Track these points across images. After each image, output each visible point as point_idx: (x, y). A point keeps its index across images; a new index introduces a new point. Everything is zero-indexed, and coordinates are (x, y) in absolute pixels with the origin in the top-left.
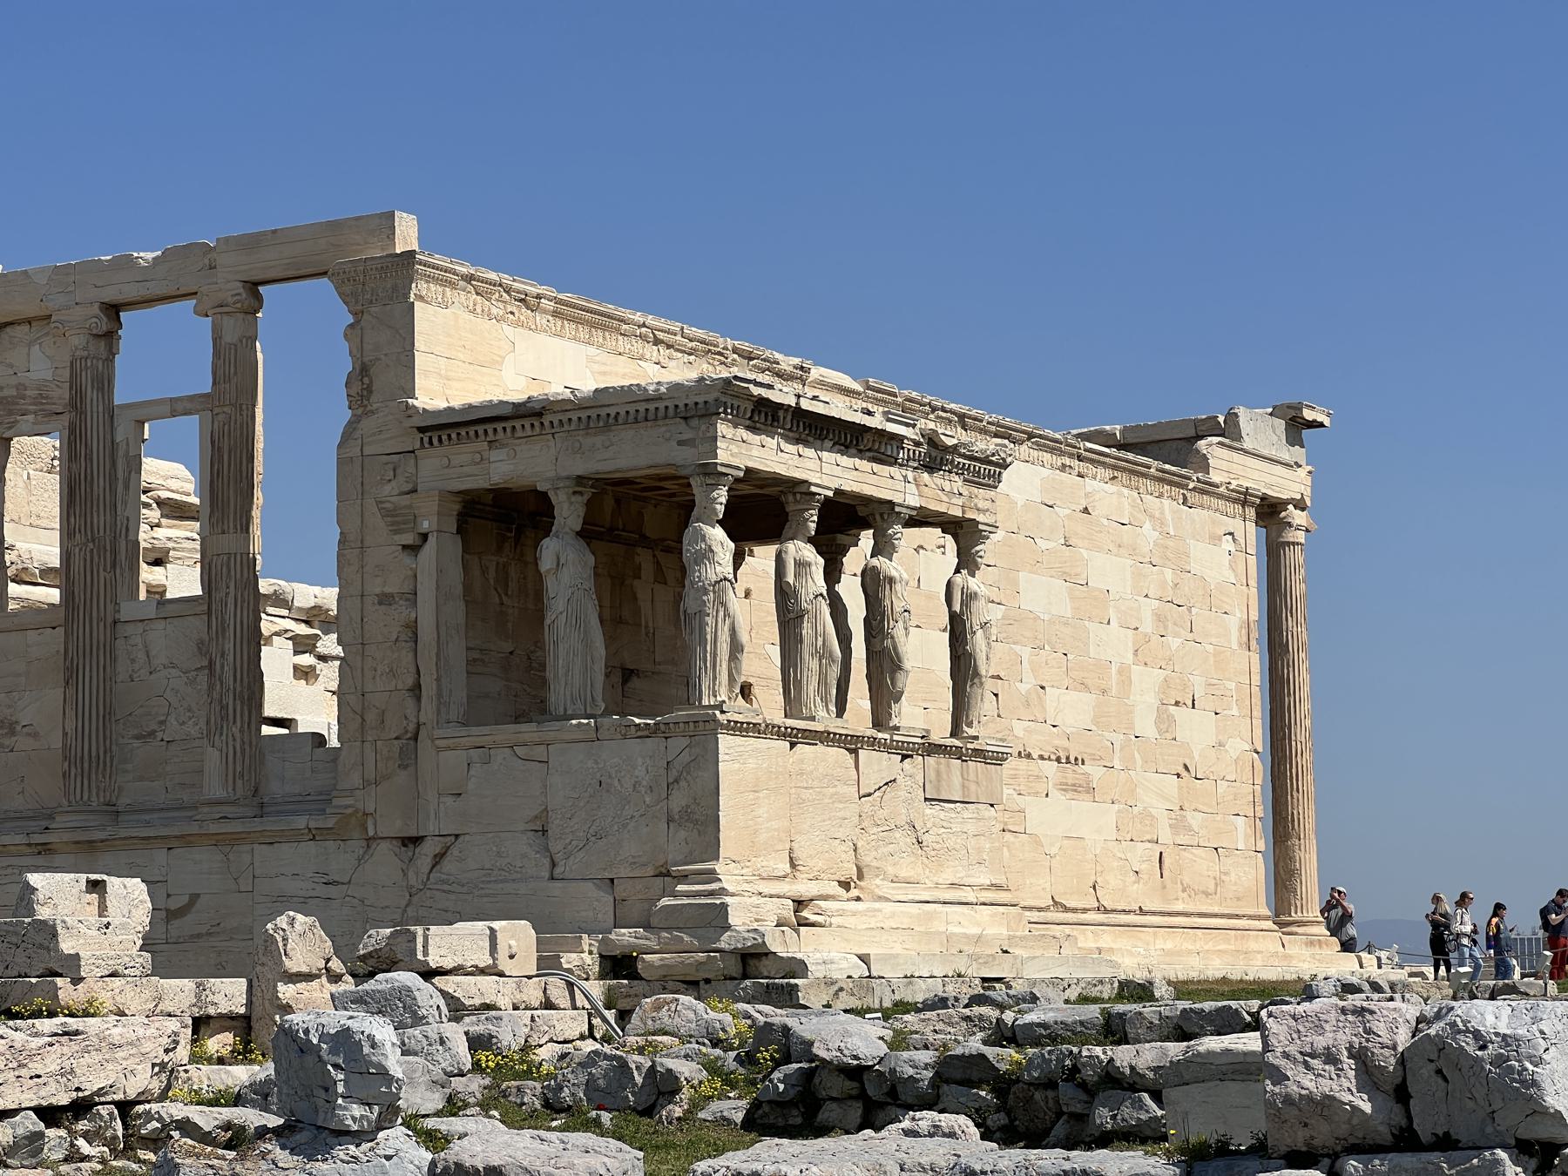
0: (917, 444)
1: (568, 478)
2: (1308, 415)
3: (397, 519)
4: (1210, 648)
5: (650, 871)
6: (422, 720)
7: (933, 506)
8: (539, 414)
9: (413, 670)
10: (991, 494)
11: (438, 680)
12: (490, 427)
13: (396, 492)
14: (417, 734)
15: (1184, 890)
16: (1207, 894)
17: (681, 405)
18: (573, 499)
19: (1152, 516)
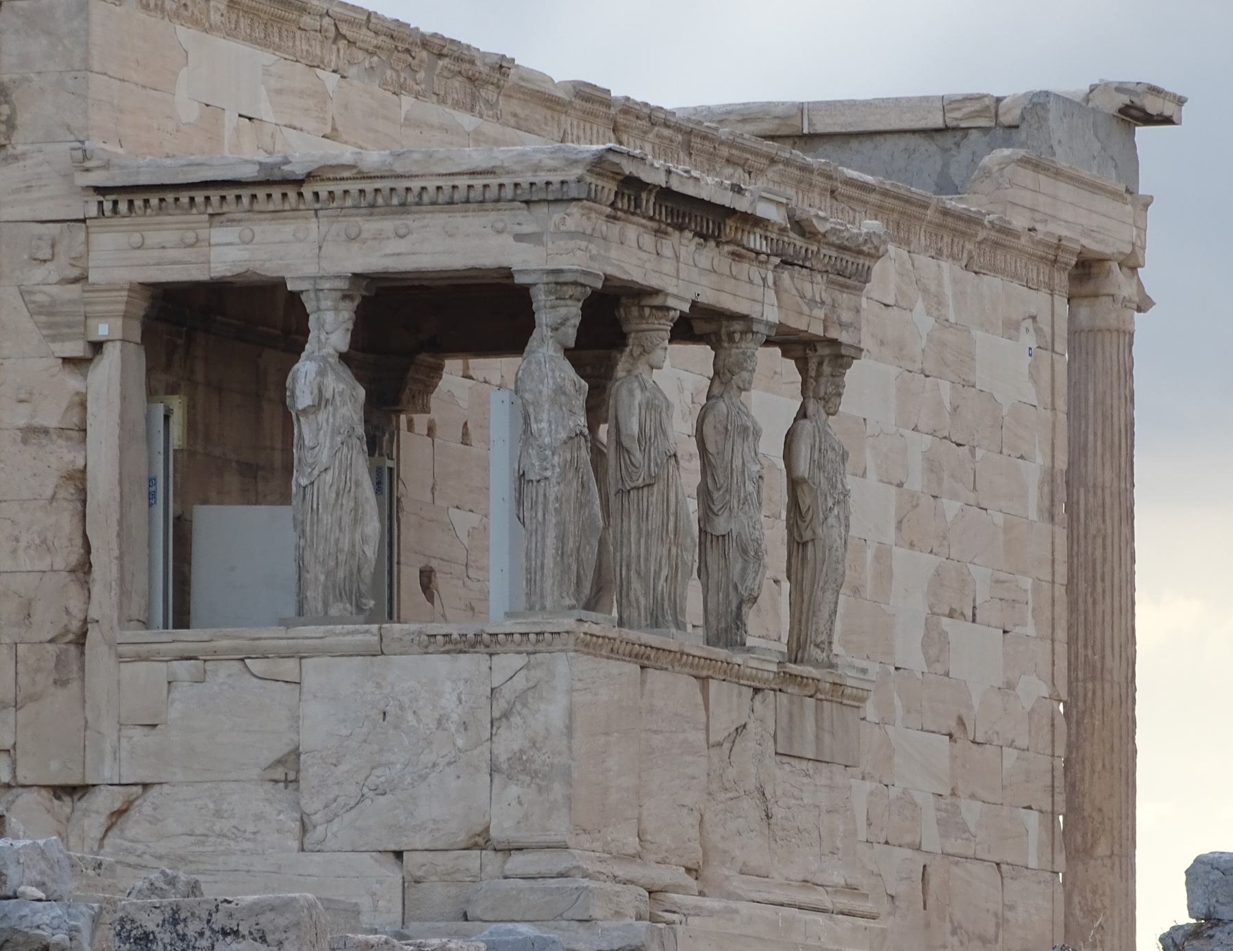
0: (783, 230)
1: (338, 277)
2: (1153, 106)
3: (51, 319)
4: (999, 518)
5: (462, 838)
6: (94, 613)
9: (79, 541)
12: (215, 195)
13: (55, 277)
14: (84, 634)
15: (954, 933)
16: (984, 940)
17: (526, 186)
18: (342, 305)
19: (925, 291)
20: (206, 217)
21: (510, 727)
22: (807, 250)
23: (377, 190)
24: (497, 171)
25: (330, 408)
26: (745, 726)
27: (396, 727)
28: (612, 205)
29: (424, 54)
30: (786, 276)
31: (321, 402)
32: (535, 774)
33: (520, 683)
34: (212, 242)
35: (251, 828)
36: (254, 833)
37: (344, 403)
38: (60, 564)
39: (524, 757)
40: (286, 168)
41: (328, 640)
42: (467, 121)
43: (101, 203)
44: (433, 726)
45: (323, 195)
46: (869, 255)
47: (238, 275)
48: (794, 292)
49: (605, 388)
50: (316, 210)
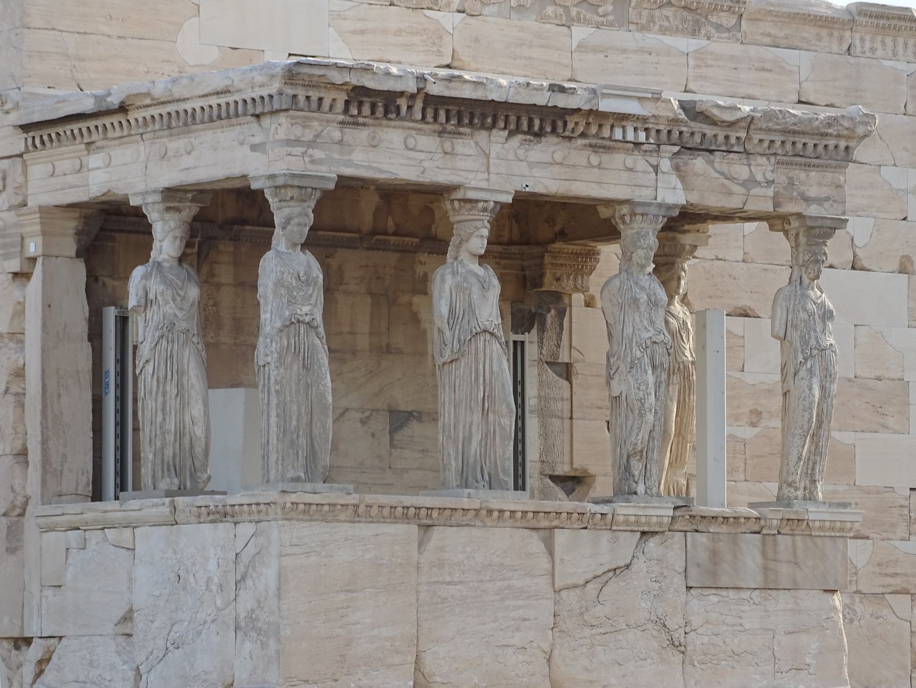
0: (675, 121)
1: (154, 192)
6: (29, 492)
7: (714, 201)
8: (123, 109)
10: (829, 175)
11: (44, 442)
12: (83, 125)
18: (167, 216)
20: (83, 146)
21: (245, 588)
22: (727, 137)
23: (169, 114)
24: (232, 89)
25: (155, 307)
26: (627, 566)
27: (184, 589)
28: (346, 111)
30: (699, 163)
31: (147, 302)
32: (259, 631)
33: (251, 549)
34: (90, 167)
35: (108, 677)
36: (110, 681)
37: (167, 303)
38: (8, 451)
39: (254, 616)
40: (109, 99)
41: (145, 512)
42: (684, 43)
43: (26, 139)
44: (204, 588)
45: (140, 120)
46: (838, 136)
47: (104, 194)
48: (717, 175)
49: (673, 264)
50: (142, 134)
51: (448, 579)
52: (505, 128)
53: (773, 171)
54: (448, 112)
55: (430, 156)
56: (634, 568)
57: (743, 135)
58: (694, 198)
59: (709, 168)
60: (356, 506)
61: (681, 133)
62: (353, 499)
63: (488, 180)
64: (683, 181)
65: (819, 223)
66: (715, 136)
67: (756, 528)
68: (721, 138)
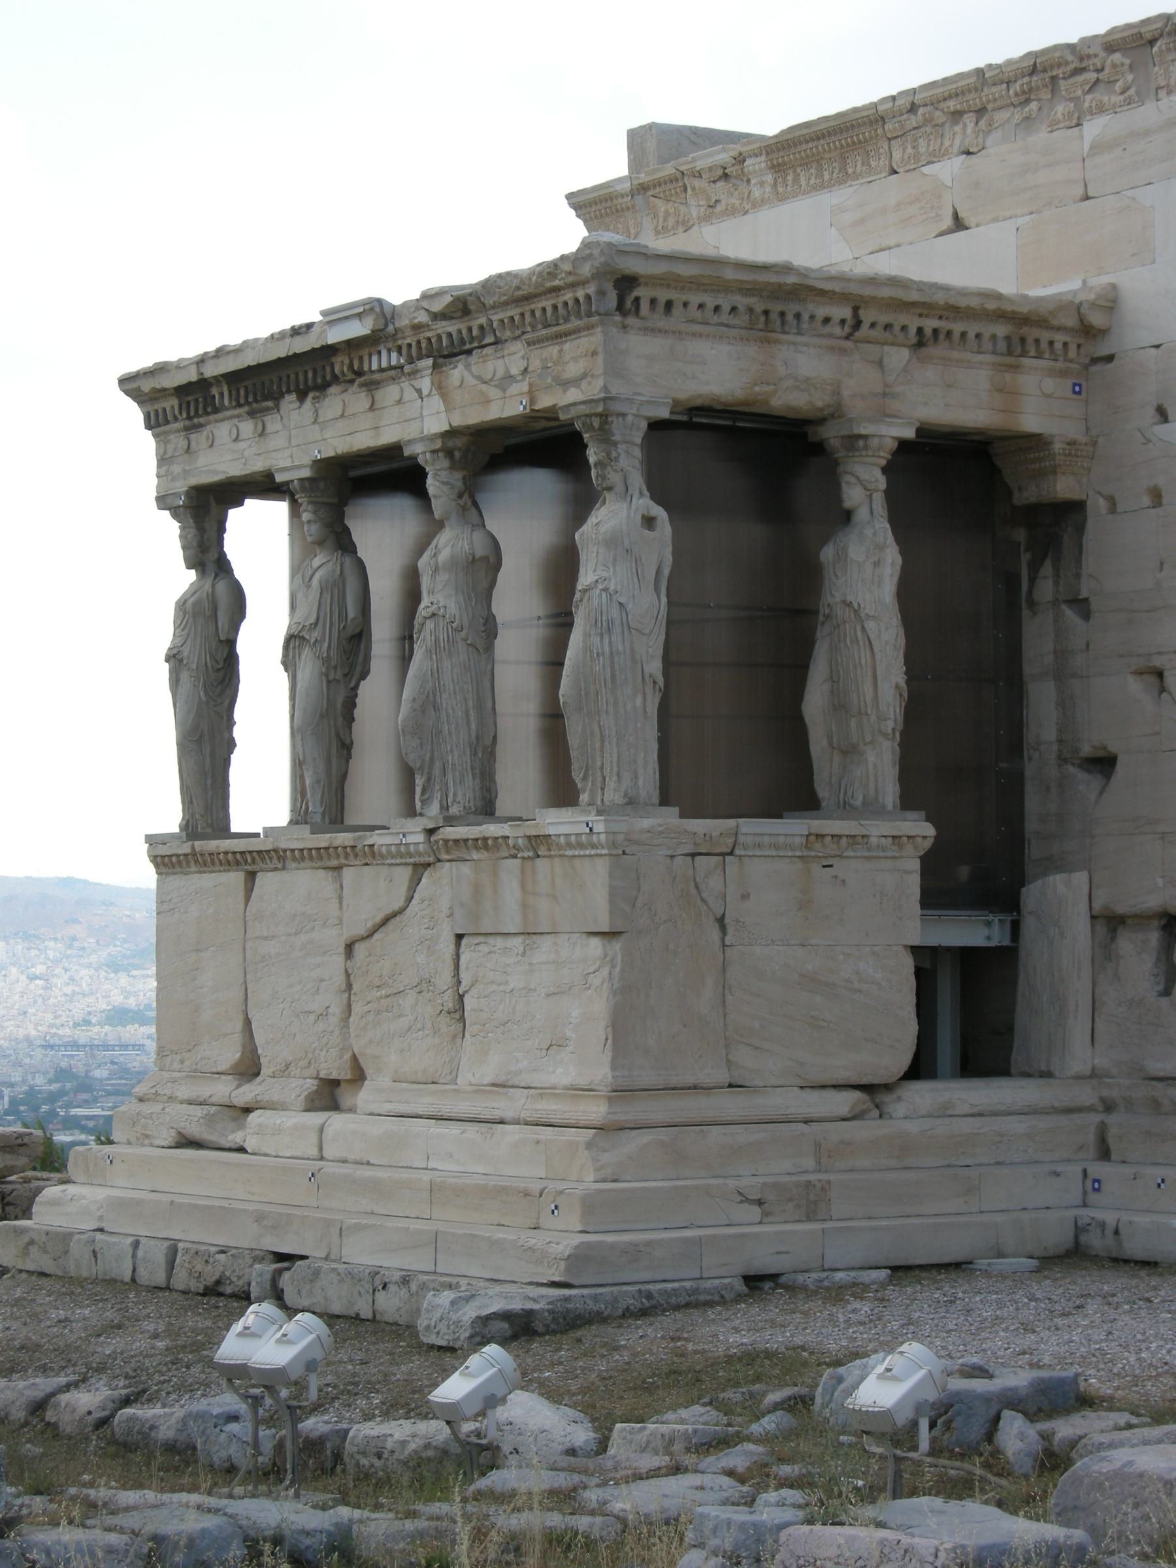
22: (470, 329)
29: (1117, 57)
30: (457, 372)
48: (475, 382)
51: (265, 934)
52: (289, 391)
53: (523, 357)
54: (246, 387)
55: (248, 443)
56: (408, 911)
57: (483, 320)
58: (458, 421)
59: (466, 374)
60: (194, 854)
61: (429, 339)
62: (186, 848)
63: (291, 456)
64: (444, 401)
65: (573, 413)
66: (460, 332)
67: (513, 852)
68: (464, 332)
